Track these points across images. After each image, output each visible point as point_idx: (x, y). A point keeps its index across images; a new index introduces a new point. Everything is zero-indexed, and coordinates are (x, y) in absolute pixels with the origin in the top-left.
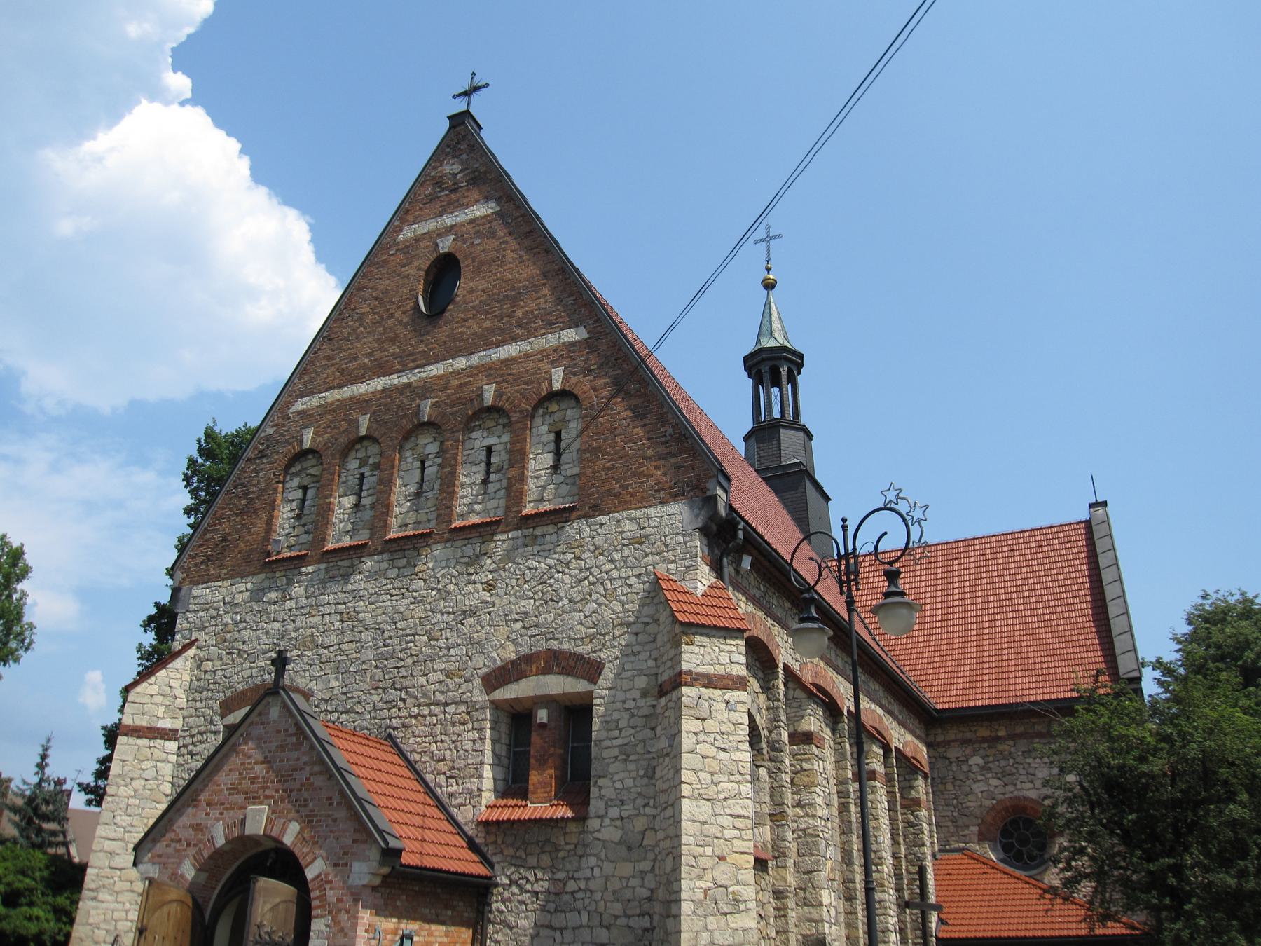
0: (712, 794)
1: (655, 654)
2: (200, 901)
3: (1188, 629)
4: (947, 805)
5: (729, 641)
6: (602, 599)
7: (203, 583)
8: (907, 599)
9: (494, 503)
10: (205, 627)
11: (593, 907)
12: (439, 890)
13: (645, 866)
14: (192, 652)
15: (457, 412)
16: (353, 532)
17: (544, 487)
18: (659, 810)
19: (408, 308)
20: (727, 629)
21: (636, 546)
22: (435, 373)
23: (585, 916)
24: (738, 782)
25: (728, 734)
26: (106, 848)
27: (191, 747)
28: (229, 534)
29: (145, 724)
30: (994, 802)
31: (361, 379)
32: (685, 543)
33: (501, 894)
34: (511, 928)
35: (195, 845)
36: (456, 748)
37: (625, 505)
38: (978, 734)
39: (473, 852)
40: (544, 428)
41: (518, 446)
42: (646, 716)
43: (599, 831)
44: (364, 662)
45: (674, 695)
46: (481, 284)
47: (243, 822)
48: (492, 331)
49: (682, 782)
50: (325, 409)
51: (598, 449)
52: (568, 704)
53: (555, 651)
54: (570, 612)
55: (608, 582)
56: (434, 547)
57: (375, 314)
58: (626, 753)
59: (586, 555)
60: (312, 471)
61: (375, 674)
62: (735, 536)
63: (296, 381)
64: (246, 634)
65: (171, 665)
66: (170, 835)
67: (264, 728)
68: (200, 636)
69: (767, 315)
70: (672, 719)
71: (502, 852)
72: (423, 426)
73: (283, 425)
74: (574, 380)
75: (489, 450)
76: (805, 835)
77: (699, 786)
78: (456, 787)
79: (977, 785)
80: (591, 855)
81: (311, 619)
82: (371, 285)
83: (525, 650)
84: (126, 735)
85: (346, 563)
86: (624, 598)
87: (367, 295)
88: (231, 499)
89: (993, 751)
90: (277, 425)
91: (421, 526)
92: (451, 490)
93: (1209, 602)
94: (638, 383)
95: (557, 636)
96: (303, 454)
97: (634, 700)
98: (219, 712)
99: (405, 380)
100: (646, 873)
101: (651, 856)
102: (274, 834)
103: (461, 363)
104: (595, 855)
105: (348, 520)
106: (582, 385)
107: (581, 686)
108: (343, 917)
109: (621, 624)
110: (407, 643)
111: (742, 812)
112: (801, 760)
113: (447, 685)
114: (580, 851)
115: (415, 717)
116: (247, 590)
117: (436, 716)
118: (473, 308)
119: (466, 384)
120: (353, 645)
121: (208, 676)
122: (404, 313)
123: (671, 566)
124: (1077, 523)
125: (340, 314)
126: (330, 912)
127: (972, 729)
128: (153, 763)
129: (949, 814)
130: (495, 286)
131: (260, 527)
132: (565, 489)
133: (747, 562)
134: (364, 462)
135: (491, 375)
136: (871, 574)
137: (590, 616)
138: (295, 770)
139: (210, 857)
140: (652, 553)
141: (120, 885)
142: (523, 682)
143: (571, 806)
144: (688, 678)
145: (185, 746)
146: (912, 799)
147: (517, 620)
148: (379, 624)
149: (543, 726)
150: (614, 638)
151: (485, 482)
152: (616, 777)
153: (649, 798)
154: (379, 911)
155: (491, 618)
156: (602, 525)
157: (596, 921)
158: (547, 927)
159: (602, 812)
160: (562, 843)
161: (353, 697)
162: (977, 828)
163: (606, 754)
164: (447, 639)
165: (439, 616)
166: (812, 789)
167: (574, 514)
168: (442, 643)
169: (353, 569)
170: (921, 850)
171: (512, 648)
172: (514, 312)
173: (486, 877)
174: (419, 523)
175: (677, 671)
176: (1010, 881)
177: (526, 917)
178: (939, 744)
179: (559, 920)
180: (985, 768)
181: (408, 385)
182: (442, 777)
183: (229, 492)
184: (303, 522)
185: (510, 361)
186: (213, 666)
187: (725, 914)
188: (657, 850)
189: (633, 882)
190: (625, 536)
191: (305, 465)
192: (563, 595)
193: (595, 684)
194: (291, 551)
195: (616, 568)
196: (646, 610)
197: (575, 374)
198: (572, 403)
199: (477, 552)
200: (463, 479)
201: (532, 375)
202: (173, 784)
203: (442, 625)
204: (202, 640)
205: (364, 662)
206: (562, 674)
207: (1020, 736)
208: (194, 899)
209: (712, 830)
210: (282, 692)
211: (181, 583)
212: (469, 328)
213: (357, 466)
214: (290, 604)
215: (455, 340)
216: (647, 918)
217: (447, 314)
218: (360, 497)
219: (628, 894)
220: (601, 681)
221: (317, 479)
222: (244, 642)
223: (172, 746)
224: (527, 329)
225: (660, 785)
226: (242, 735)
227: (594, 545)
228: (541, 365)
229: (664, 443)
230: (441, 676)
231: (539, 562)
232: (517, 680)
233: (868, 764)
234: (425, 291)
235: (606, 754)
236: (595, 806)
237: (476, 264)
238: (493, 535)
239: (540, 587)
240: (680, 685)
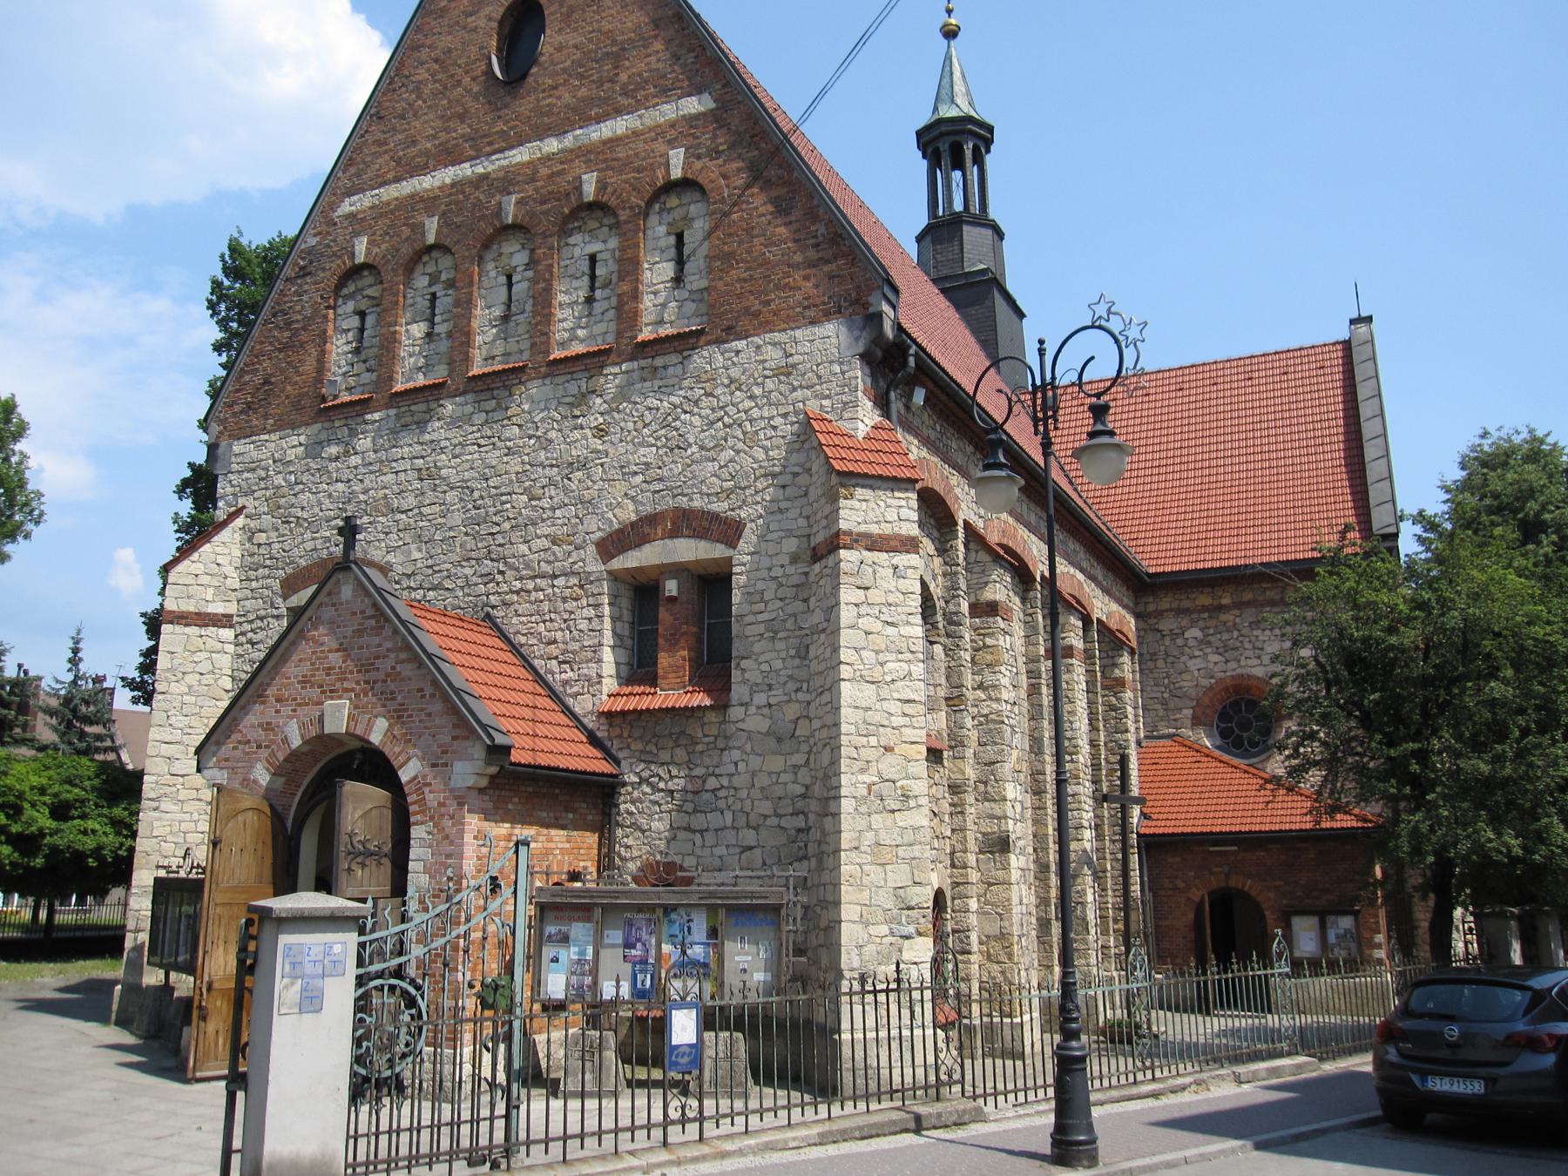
0: (877, 676)
2: (280, 809)
3: (1459, 475)
4: (1156, 685)
5: (897, 494)
6: (740, 445)
7: (245, 437)
8: (1116, 440)
9: (600, 328)
10: (254, 491)
11: (738, 806)
12: (557, 791)
13: (799, 759)
14: (240, 521)
15: (549, 210)
16: (426, 368)
17: (664, 305)
18: (814, 695)
19: (479, 72)
20: (894, 479)
21: (782, 378)
22: (518, 159)
23: (729, 816)
25: (897, 605)
26: (163, 753)
27: (250, 635)
28: (272, 375)
29: (192, 609)
30: (1213, 681)
31: (423, 169)
32: (843, 373)
33: (629, 794)
34: (643, 832)
35: (266, 747)
36: (568, 628)
37: (767, 326)
38: (1197, 602)
39: (595, 747)
40: (662, 230)
42: (797, 586)
43: (743, 720)
44: (451, 528)
45: (830, 561)
46: (572, 38)
47: (321, 720)
48: (589, 101)
49: (841, 662)
50: (380, 211)
51: (732, 254)
52: (702, 572)
53: (685, 510)
54: (701, 461)
55: (747, 423)
56: (530, 385)
57: (435, 81)
58: (773, 630)
59: (719, 391)
60: (369, 292)
61: (465, 542)
62: (905, 363)
65: (215, 538)
66: (236, 737)
67: (336, 610)
68: (249, 502)
69: (947, 73)
70: (828, 589)
71: (628, 747)
72: (506, 230)
73: (328, 233)
74: (698, 165)
75: (593, 259)
76: (987, 722)
77: (861, 667)
78: (570, 674)
79: (1194, 661)
80: (734, 748)
81: (382, 478)
82: (428, 42)
83: (648, 509)
84: (171, 622)
85: (422, 407)
86: (767, 443)
88: (270, 330)
89: (1214, 622)
91: (512, 359)
92: (546, 311)
93: (1490, 442)
95: (686, 491)
96: (356, 271)
97: (782, 566)
98: (280, 592)
99: (480, 170)
100: (799, 767)
101: (804, 747)
102: (359, 731)
103: (552, 145)
104: (739, 748)
105: (420, 353)
106: (710, 172)
107: (718, 551)
108: (448, 823)
109: (765, 476)
110: (503, 503)
112: (984, 635)
113: (554, 553)
114: (721, 744)
115: (518, 592)
116: (301, 444)
117: (542, 590)
118: (564, 70)
119: (560, 173)
120: (436, 508)
121: (262, 551)
122: (474, 79)
123: (826, 402)
124: (1334, 344)
125: (390, 84)
126: (432, 818)
127: (1192, 596)
128: (207, 655)
129: (1159, 695)
130: (590, 40)
131: (309, 365)
132: (690, 307)
133: (919, 396)
134: (434, 279)
135: (590, 161)
136: (1074, 410)
137: (726, 466)
138: (377, 658)
139: (285, 760)
140: (801, 387)
141: (183, 794)
142: (647, 548)
143: (708, 692)
144: (848, 540)
145: (243, 634)
146: (1116, 679)
147: (636, 473)
148: (466, 481)
149: (672, 599)
150: (757, 492)
151: (590, 300)
152: (762, 658)
153: (801, 681)
154: (488, 816)
155: (604, 471)
156: (738, 352)
157: (742, 822)
158: (685, 829)
159: (746, 699)
160: (700, 735)
161: (440, 571)
162: (1191, 711)
163: (749, 631)
164: (551, 498)
165: (540, 469)
166: (997, 669)
167: (703, 339)
168: (545, 503)
169: (429, 414)
170: (1124, 736)
171: (631, 507)
172: (617, 74)
173: (611, 775)
174: (509, 354)
175: (834, 531)
176: (1227, 770)
177: (660, 819)
178: (1150, 615)
179: (698, 821)
180: (1204, 642)
182: (554, 662)
183: (266, 322)
184: (363, 357)
186: (268, 538)
187: (893, 811)
188: (812, 741)
189: (784, 778)
190: (767, 365)
191: (360, 284)
192: (691, 440)
193: (735, 548)
194: (351, 394)
195: (757, 405)
196: (795, 458)
197: (699, 157)
198: (697, 195)
200: (561, 298)
201: (644, 159)
202: (233, 679)
203: (545, 481)
204: (251, 507)
205: (451, 528)
206: (693, 537)
207: (1248, 604)
208: (271, 807)
210: (353, 566)
211: (218, 437)
212: (559, 98)
213: (426, 283)
214: (355, 460)
215: (542, 114)
216: (801, 817)
217: (530, 79)
218: (432, 324)
219: (779, 791)
220: (742, 544)
221: (376, 302)
222: (303, 508)
223: (228, 634)
224: (635, 99)
225: (815, 667)
226: (310, 619)
227: (729, 377)
228: (655, 145)
229: (816, 246)
230: (546, 543)
231: (661, 401)
232: (639, 546)
233: (1063, 638)
234: (499, 50)
235: (749, 631)
236: (738, 692)
238: (602, 367)
239: (663, 432)
240: (838, 547)
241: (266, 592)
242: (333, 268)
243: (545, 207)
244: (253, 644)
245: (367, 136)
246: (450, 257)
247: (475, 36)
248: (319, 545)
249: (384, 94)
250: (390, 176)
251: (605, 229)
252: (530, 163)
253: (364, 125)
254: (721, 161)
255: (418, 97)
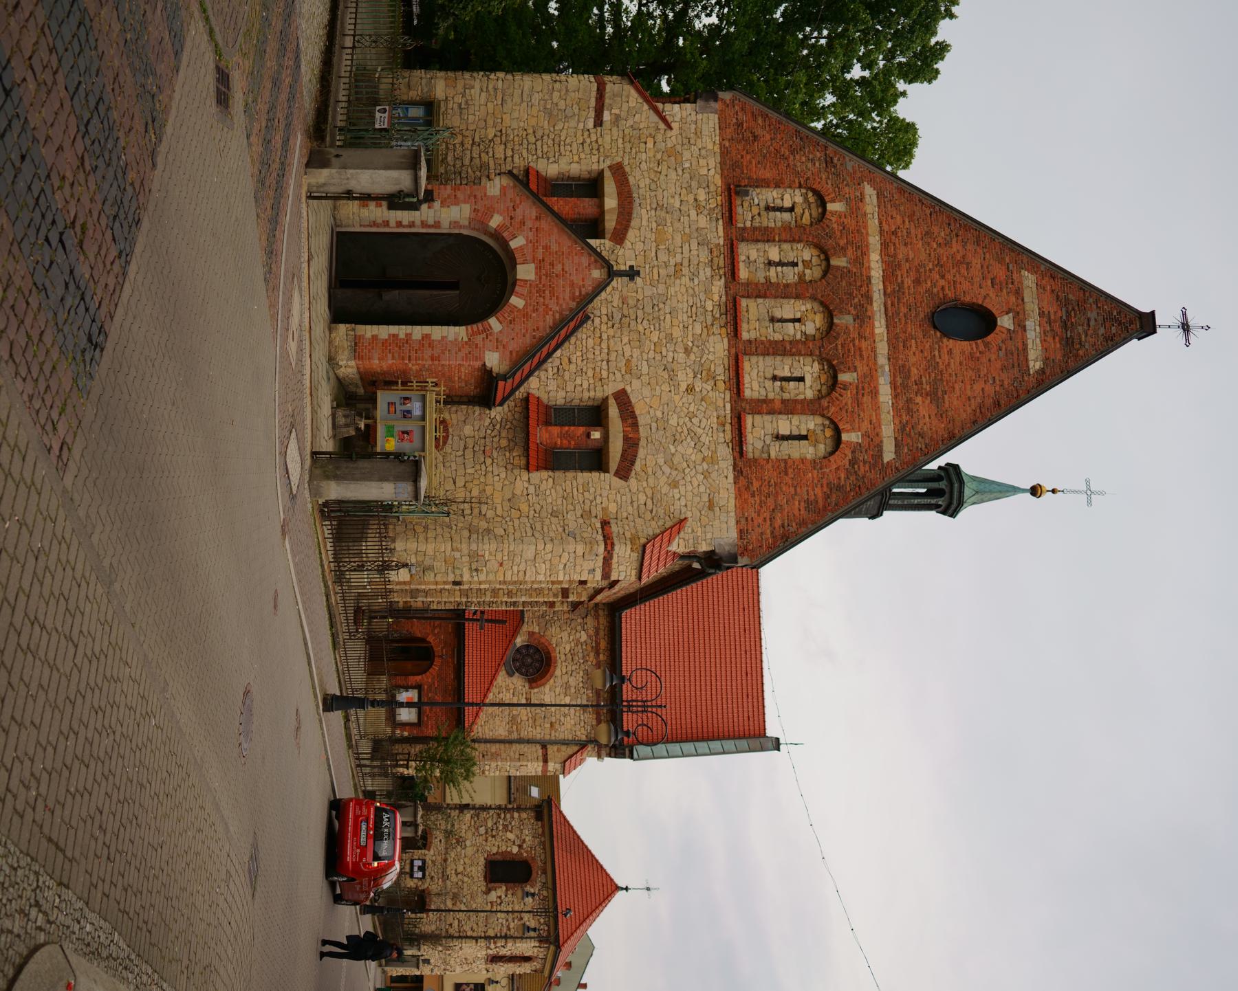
1: (631, 518)
11: (476, 476)
14: (662, 126)
16: (749, 262)
22: (877, 324)
24: (545, 574)
27: (588, 141)
37: (739, 495)
40: (811, 426)
41: (799, 407)
59: (705, 466)
60: (807, 213)
62: (711, 567)
63: (895, 185)
64: (673, 175)
72: (830, 315)
75: (801, 379)
83: (642, 421)
84: (598, 89)
85: (722, 264)
87: (969, 247)
90: (854, 172)
92: (771, 350)
94: (836, 504)
96: (822, 203)
101: (505, 514)
103: (882, 348)
106: (842, 460)
107: (614, 465)
108: (467, 349)
111: (528, 575)
114: (509, 466)
115: (600, 337)
119: (861, 356)
120: (656, 277)
121: (642, 145)
122: (943, 288)
126: (470, 340)
132: (759, 445)
134: (807, 264)
149: (588, 435)
151: (775, 378)
152: (553, 491)
157: (468, 478)
167: (737, 455)
179: (469, 453)
181: (868, 298)
185: (875, 393)
191: (813, 206)
197: (853, 452)
198: (829, 449)
199: (718, 378)
203: (664, 354)
209: (517, 560)
214: (693, 213)
215: (904, 342)
223: (590, 124)
224: (904, 407)
230: (627, 354)
236: (536, 476)
237: (978, 354)
241: (614, 151)
242: (827, 187)
243: (840, 347)
244: (582, 144)
245: (919, 204)
246: (820, 276)
247: (976, 286)
248: (641, 191)
249: (948, 217)
250: (886, 227)
251: (819, 387)
252: (873, 334)
253: (928, 202)
254: (847, 466)
255: (939, 245)
